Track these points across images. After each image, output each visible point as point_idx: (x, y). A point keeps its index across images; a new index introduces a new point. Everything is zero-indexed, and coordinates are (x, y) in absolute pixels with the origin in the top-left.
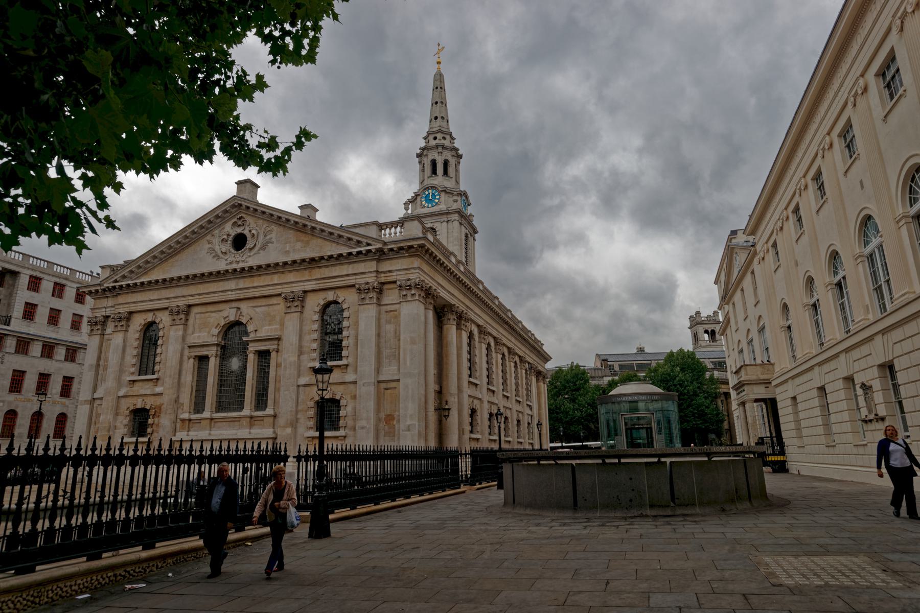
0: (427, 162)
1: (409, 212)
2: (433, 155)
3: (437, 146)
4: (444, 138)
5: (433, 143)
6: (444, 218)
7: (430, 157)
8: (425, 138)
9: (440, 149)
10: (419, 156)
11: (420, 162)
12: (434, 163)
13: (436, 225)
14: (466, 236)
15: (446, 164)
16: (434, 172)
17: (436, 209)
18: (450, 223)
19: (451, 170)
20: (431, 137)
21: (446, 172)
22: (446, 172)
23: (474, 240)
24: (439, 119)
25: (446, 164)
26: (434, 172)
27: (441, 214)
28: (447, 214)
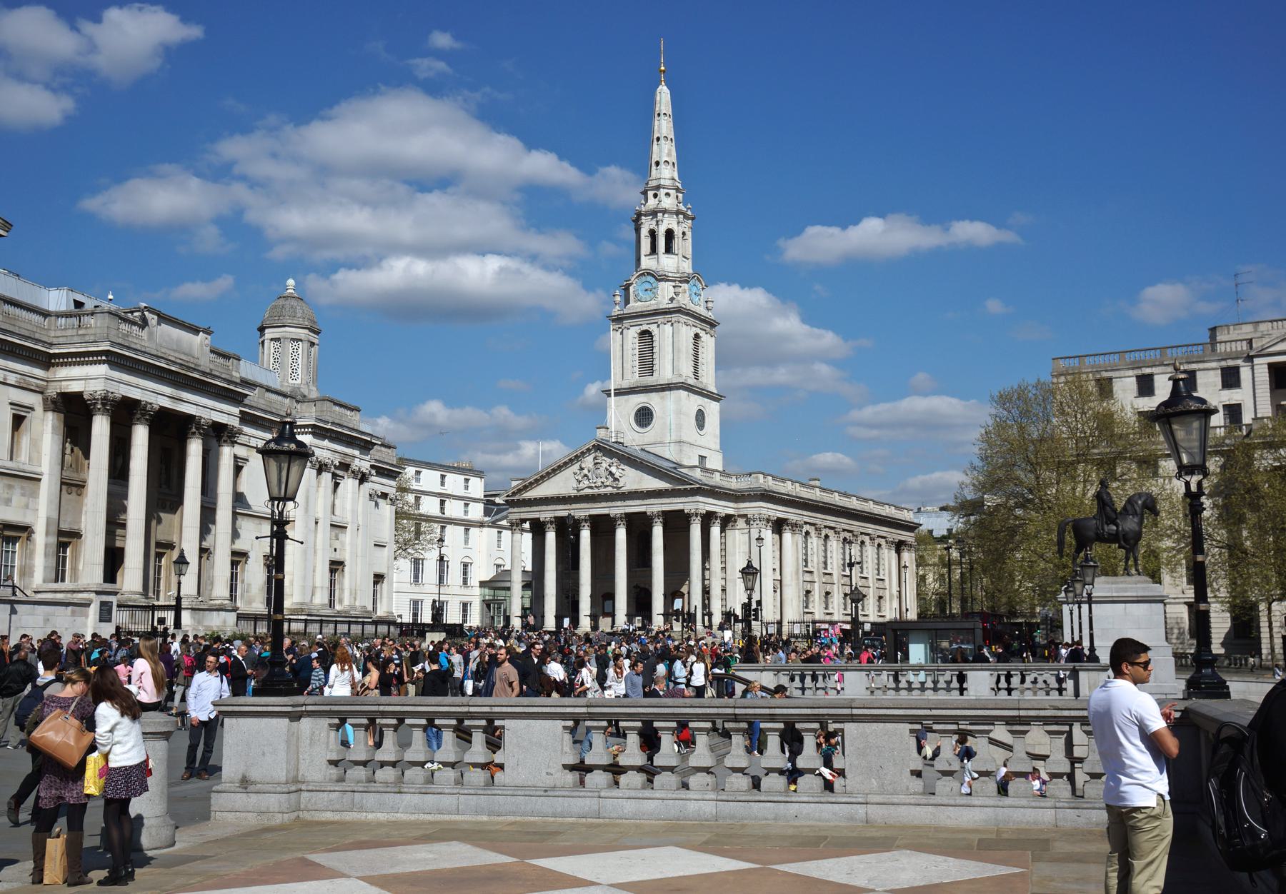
3: (654, 213)
4: (668, 194)
6: (660, 319)
9: (660, 215)
12: (653, 234)
13: (653, 328)
14: (697, 336)
15: (670, 234)
16: (654, 250)
17: (652, 305)
19: (678, 243)
21: (669, 250)
22: (669, 250)
24: (662, 166)
25: (670, 234)
26: (654, 250)
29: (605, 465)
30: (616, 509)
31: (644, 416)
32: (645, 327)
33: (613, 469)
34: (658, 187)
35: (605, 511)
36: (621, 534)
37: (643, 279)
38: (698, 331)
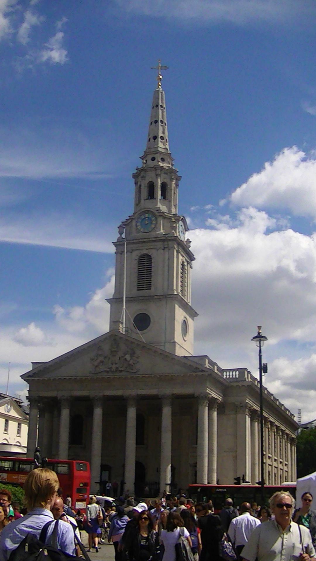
0: (144, 184)
1: (123, 236)
2: (150, 177)
4: (163, 160)
5: (151, 163)
6: (160, 244)
7: (148, 179)
8: (142, 158)
9: (159, 172)
10: (135, 176)
11: (136, 183)
15: (164, 187)
18: (166, 250)
20: (150, 157)
23: (191, 267)
25: (164, 187)
26: (151, 195)
27: (157, 240)
28: (164, 241)
29: (120, 354)
30: (132, 392)
31: (142, 321)
32: (145, 252)
33: (128, 357)
34: (157, 152)
35: (119, 393)
36: (132, 413)
37: (147, 215)
38: (184, 260)
